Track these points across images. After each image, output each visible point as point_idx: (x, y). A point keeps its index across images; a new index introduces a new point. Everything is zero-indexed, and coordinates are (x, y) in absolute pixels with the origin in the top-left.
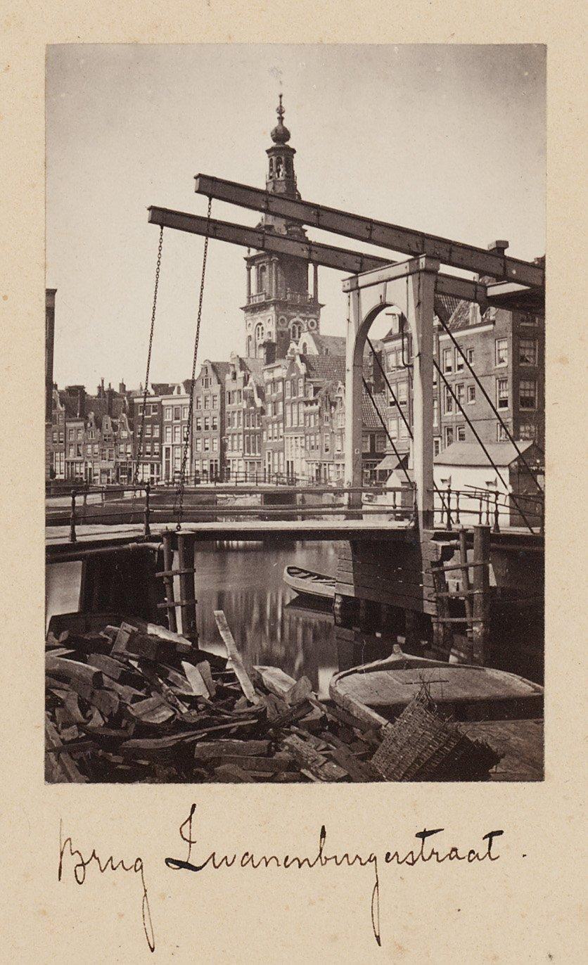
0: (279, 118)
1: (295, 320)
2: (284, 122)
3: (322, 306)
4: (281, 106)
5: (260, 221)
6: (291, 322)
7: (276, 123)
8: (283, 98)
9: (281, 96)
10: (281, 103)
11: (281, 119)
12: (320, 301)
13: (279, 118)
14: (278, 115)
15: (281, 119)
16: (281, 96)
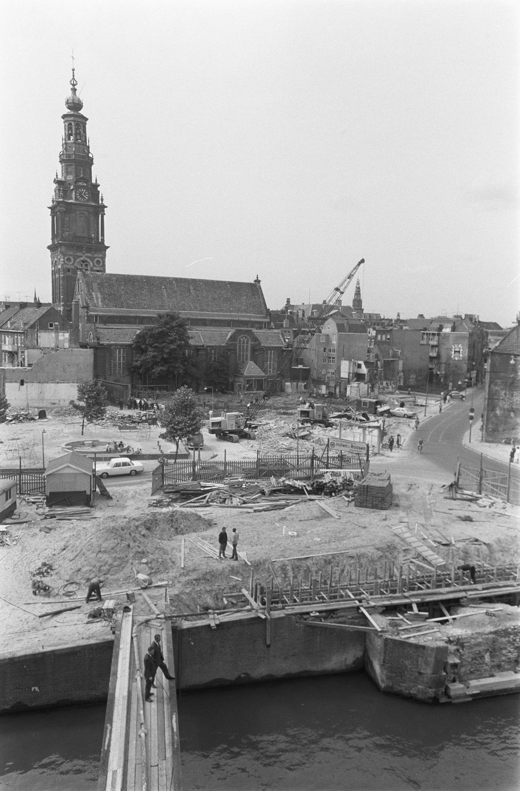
0: (72, 89)
1: (82, 259)
2: (77, 92)
3: (108, 247)
4: (74, 79)
5: (56, 177)
6: (78, 261)
7: (70, 94)
8: (75, 71)
9: (73, 70)
10: (74, 76)
11: (74, 90)
12: (106, 244)
13: (72, 89)
14: (71, 87)
15: (74, 90)
16: (73, 70)
